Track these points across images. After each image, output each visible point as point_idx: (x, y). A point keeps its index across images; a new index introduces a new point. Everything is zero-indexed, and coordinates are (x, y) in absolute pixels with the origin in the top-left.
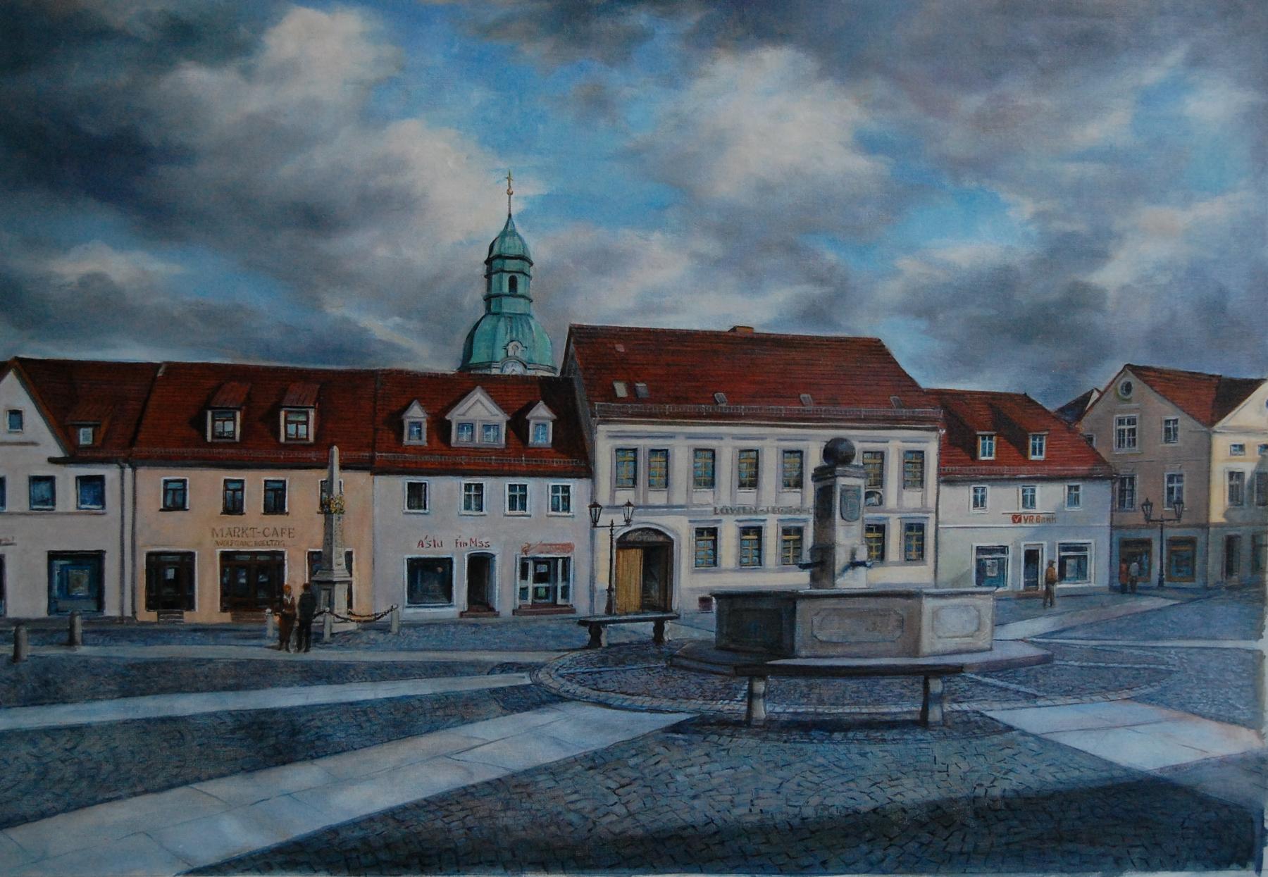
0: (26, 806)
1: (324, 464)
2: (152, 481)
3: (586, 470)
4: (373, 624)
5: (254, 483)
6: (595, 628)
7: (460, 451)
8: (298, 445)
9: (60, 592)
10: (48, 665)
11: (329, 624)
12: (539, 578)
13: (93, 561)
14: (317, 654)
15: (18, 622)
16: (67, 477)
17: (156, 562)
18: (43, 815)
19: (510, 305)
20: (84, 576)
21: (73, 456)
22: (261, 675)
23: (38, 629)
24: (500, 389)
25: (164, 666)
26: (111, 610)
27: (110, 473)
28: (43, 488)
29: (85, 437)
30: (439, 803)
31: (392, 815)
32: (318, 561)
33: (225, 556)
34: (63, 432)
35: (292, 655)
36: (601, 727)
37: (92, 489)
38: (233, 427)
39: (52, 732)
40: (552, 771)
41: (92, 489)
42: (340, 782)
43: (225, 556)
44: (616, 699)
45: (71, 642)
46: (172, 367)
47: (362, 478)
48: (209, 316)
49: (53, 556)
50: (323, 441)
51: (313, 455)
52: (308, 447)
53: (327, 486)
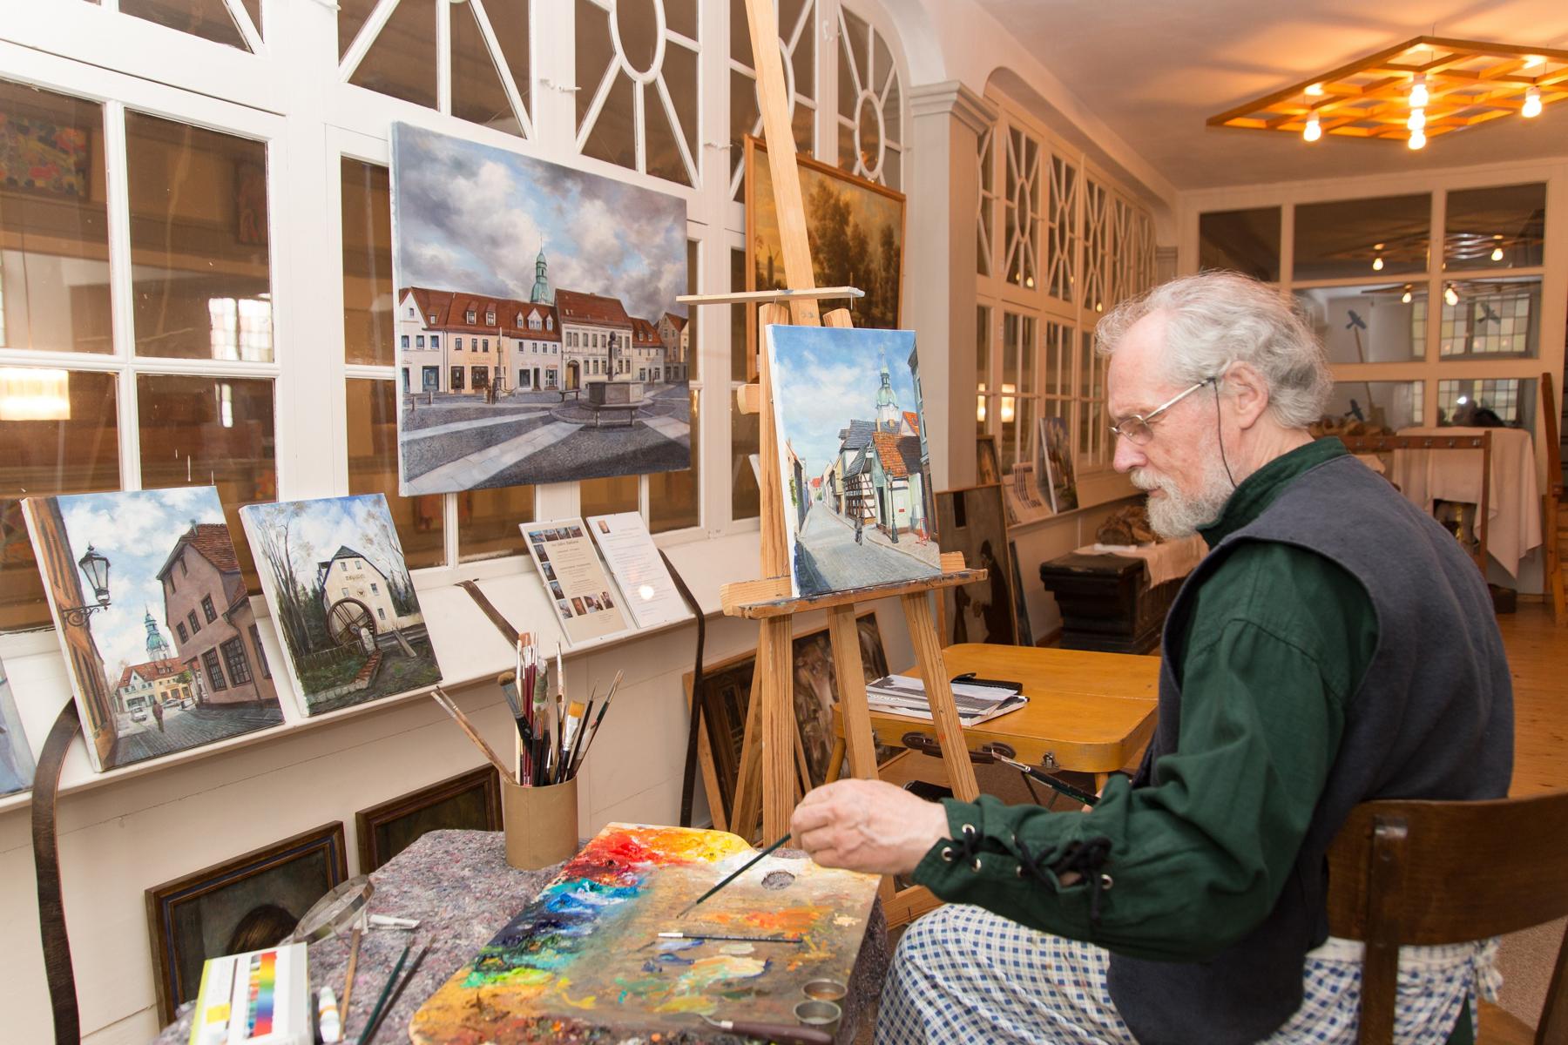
0: (418, 472)
1: (498, 334)
2: (452, 337)
3: (560, 340)
4: (511, 394)
5: (480, 339)
6: (563, 394)
7: (531, 331)
8: (491, 326)
9: (426, 382)
10: (423, 412)
11: (501, 394)
12: (551, 377)
13: (435, 369)
14: (498, 405)
15: (414, 395)
16: (428, 335)
17: (454, 370)
18: (422, 474)
19: (542, 280)
20: (433, 375)
21: (429, 329)
22: (482, 413)
23: (420, 397)
24: (542, 309)
25: (456, 411)
26: (441, 390)
27: (439, 334)
28: (421, 339)
29: (433, 320)
30: (529, 459)
31: (517, 465)
32: (497, 369)
33: (473, 368)
34: (427, 318)
35: (491, 406)
36: (565, 430)
37: (435, 338)
38: (474, 319)
39: (424, 439)
40: (554, 446)
41: (435, 338)
42: (503, 453)
43: (473, 368)
44: (568, 420)
45: (430, 403)
46: (457, 294)
47: (507, 339)
48: (468, 276)
49: (424, 368)
50: (497, 326)
51: (495, 330)
52: (493, 327)
53: (499, 342)
